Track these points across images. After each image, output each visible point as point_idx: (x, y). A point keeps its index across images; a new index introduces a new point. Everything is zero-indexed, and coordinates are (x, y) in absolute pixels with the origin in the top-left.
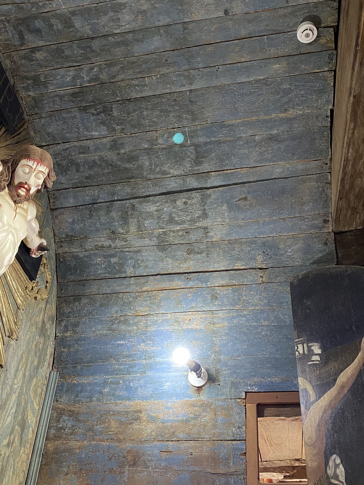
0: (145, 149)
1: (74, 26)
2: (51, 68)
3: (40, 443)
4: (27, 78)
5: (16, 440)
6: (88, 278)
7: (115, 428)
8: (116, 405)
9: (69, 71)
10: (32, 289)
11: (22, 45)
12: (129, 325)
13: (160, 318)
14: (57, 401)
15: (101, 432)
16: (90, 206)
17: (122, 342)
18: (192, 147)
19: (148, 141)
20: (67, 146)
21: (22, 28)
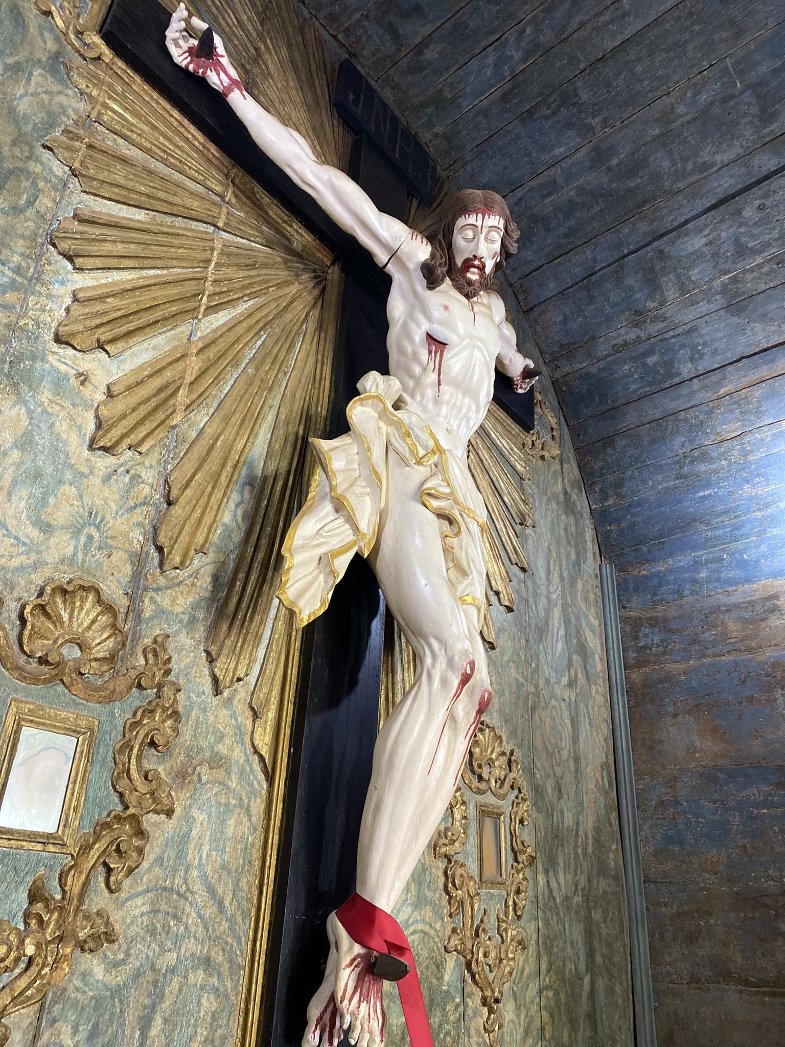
0: (656, 138)
2: (456, 67)
3: (618, 674)
5: (579, 675)
6: (617, 404)
7: (737, 631)
8: (729, 595)
9: (486, 57)
10: (533, 445)
11: (399, 50)
12: (711, 460)
13: (767, 434)
14: (624, 608)
15: (715, 643)
16: (585, 281)
17: (707, 493)
18: (748, 93)
19: (656, 120)
20: (519, 193)
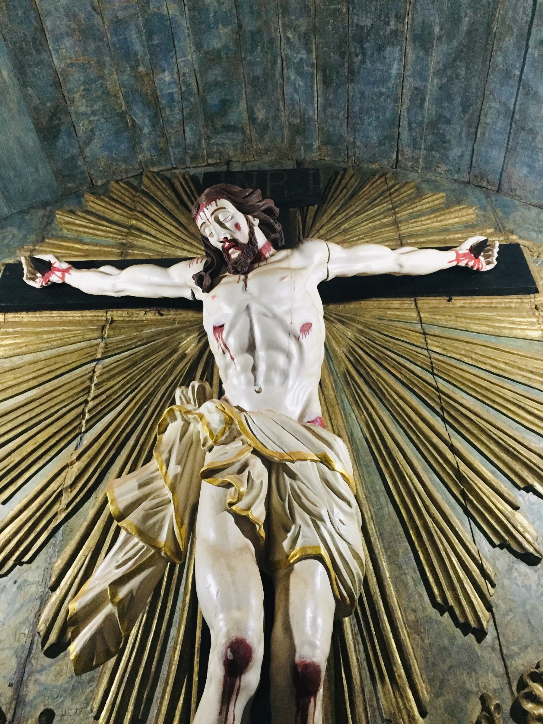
1: (219, 51)
2: (281, 103)
4: (292, 143)
9: (289, 78)
11: (244, 133)
16: (514, 126)
20: (404, 123)
21: (219, 124)
